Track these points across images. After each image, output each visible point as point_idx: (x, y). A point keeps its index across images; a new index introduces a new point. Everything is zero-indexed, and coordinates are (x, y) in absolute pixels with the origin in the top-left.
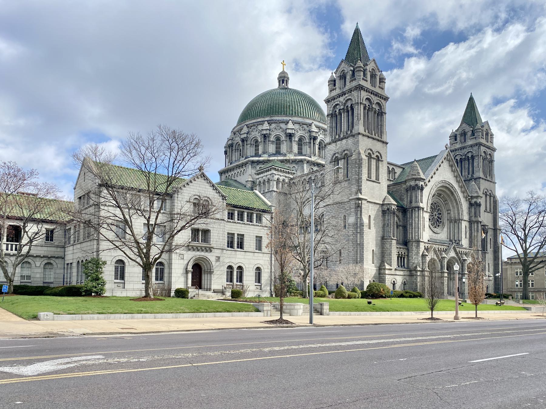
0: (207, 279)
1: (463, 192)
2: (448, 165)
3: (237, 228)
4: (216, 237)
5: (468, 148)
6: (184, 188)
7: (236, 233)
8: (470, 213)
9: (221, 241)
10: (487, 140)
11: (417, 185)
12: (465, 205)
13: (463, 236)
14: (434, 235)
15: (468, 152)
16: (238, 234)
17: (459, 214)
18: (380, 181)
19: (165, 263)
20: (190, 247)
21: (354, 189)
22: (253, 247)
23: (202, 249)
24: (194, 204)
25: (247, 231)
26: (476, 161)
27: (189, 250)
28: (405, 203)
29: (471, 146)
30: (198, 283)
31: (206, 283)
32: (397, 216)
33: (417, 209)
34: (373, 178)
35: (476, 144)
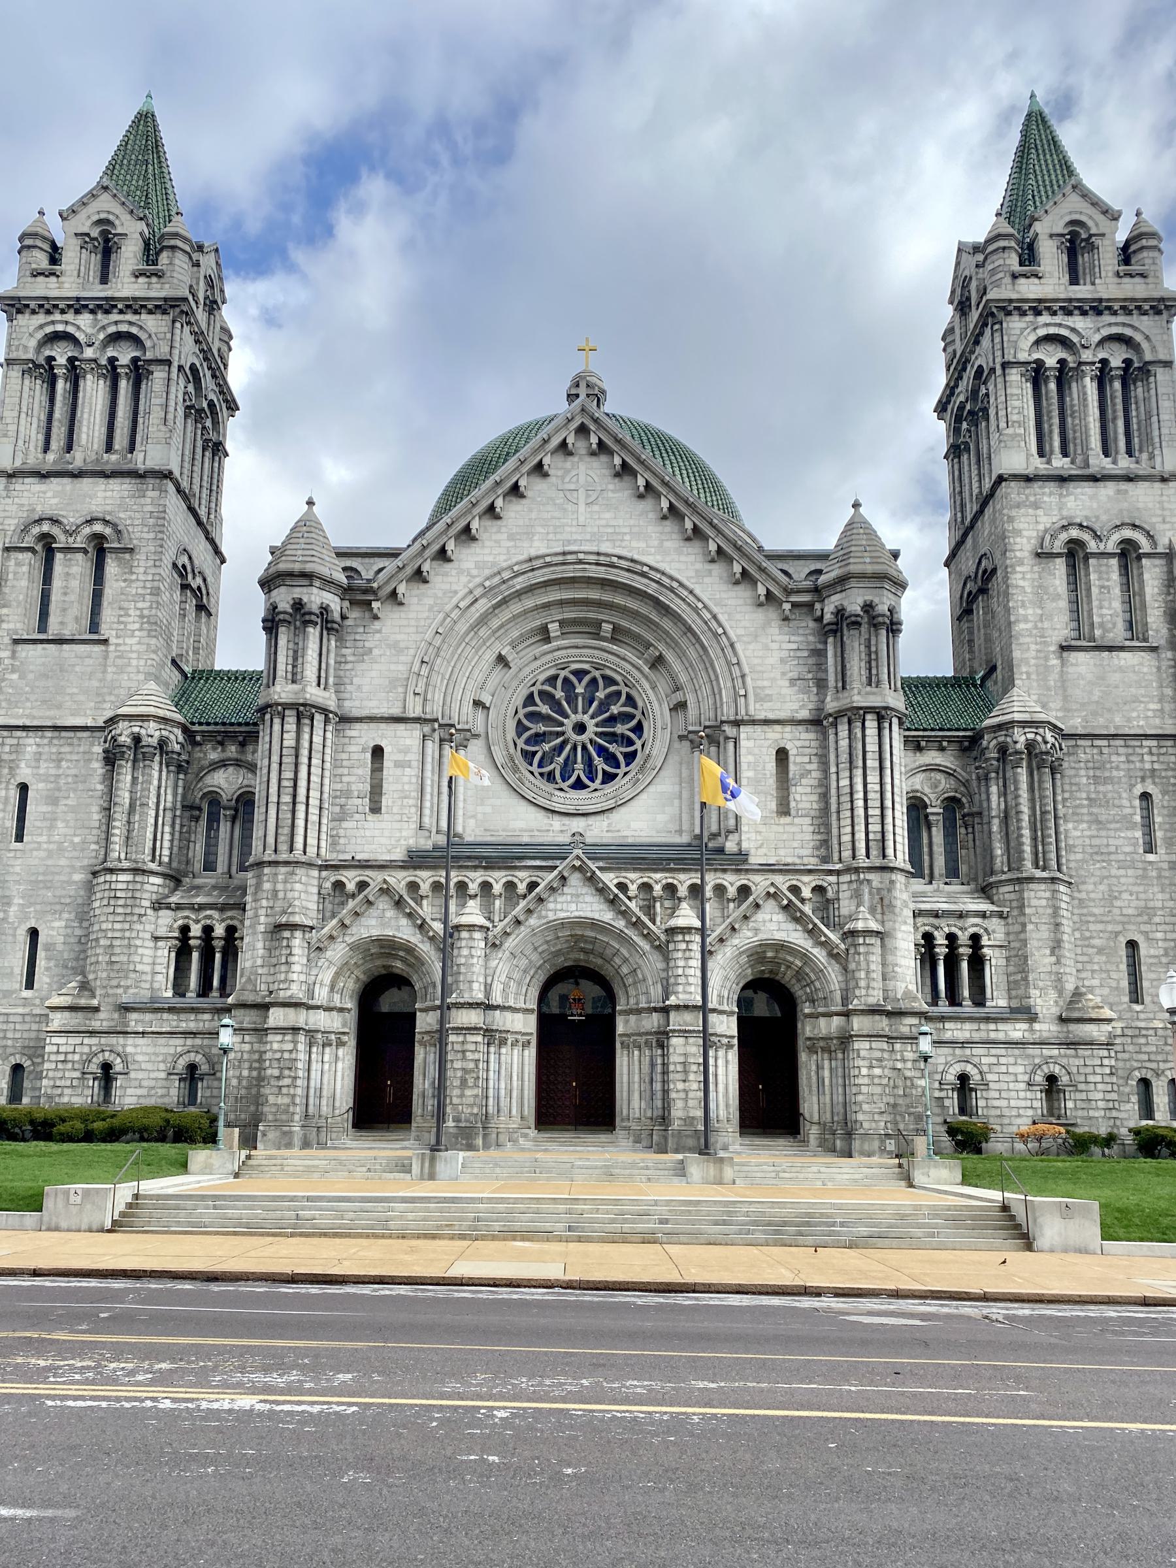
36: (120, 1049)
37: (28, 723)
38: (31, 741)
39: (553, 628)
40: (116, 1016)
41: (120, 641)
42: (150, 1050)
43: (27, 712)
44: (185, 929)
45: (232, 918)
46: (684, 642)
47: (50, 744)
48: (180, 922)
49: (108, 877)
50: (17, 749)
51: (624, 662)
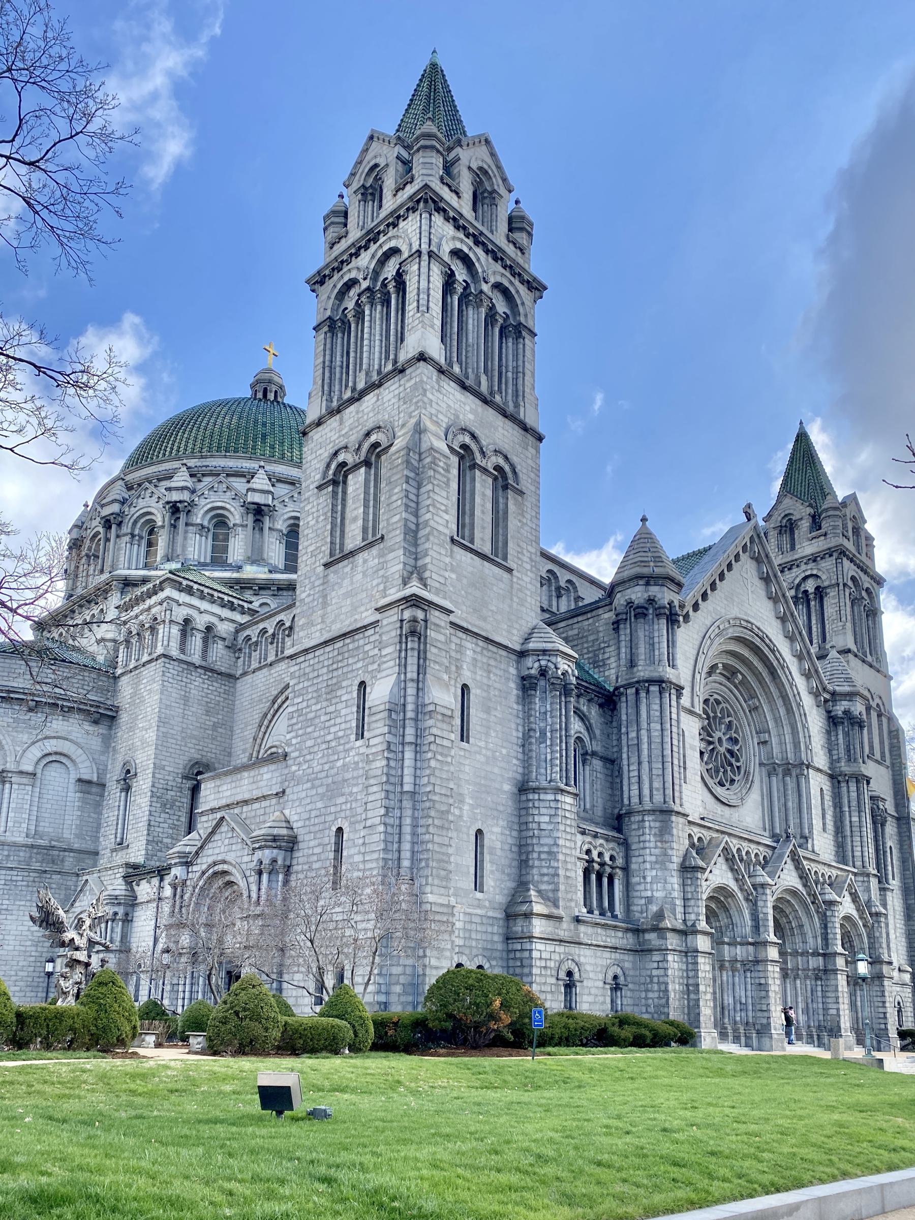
1: (807, 676)
2: (755, 573)
5: (803, 567)
8: (830, 748)
10: (858, 545)
11: (651, 601)
12: (815, 721)
13: (817, 823)
14: (719, 809)
15: (805, 578)
17: (796, 745)
18: (511, 564)
21: (396, 562)
26: (827, 602)
28: (612, 673)
29: (814, 559)
32: (583, 718)
33: (654, 689)
34: (483, 541)
35: (830, 553)
36: (576, 958)
37: (470, 628)
38: (469, 645)
39: (720, 665)
40: (572, 926)
41: (519, 575)
42: (592, 961)
43: (464, 615)
44: (588, 852)
45: (613, 849)
46: (780, 702)
47: (482, 653)
48: (585, 847)
49: (559, 797)
50: (460, 649)
51: (738, 704)
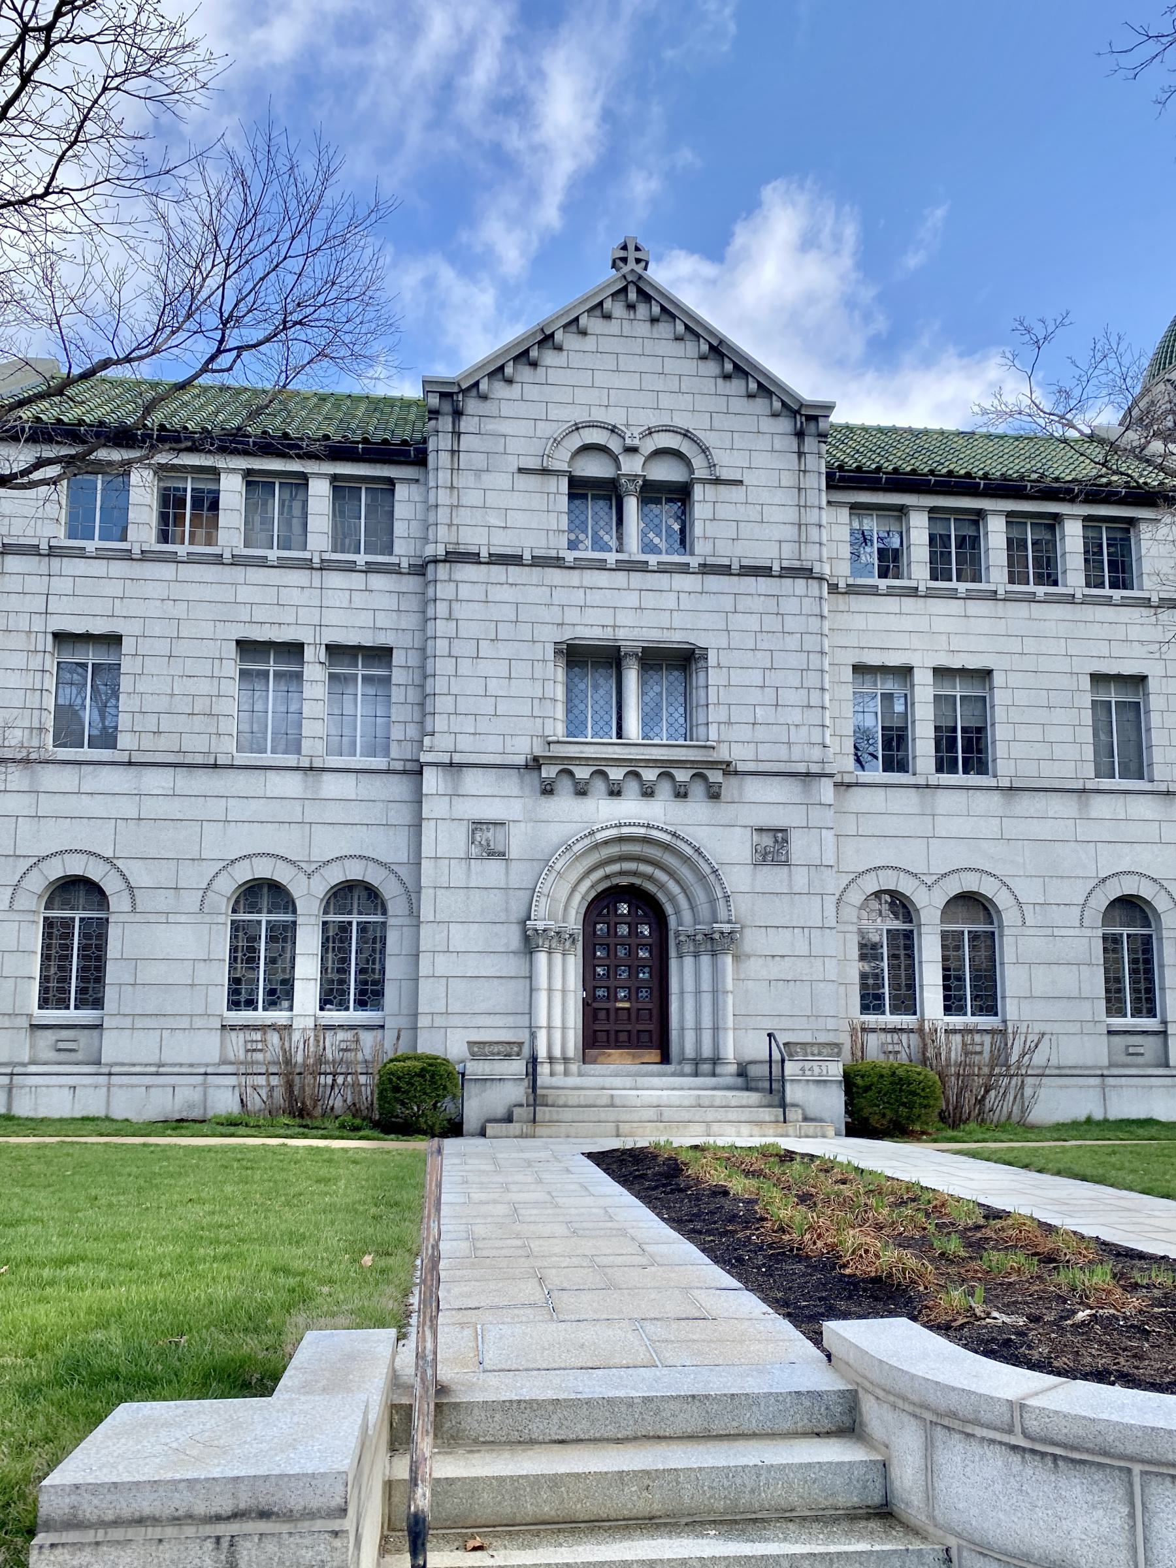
0: (698, 992)
3: (929, 630)
4: (755, 696)
6: (500, 390)
7: (923, 662)
9: (796, 716)
16: (940, 672)
19: (389, 890)
20: (549, 772)
22: (1072, 752)
23: (636, 778)
24: (579, 488)
25: (1014, 645)
27: (548, 790)
30: (630, 1014)
31: (690, 1021)
